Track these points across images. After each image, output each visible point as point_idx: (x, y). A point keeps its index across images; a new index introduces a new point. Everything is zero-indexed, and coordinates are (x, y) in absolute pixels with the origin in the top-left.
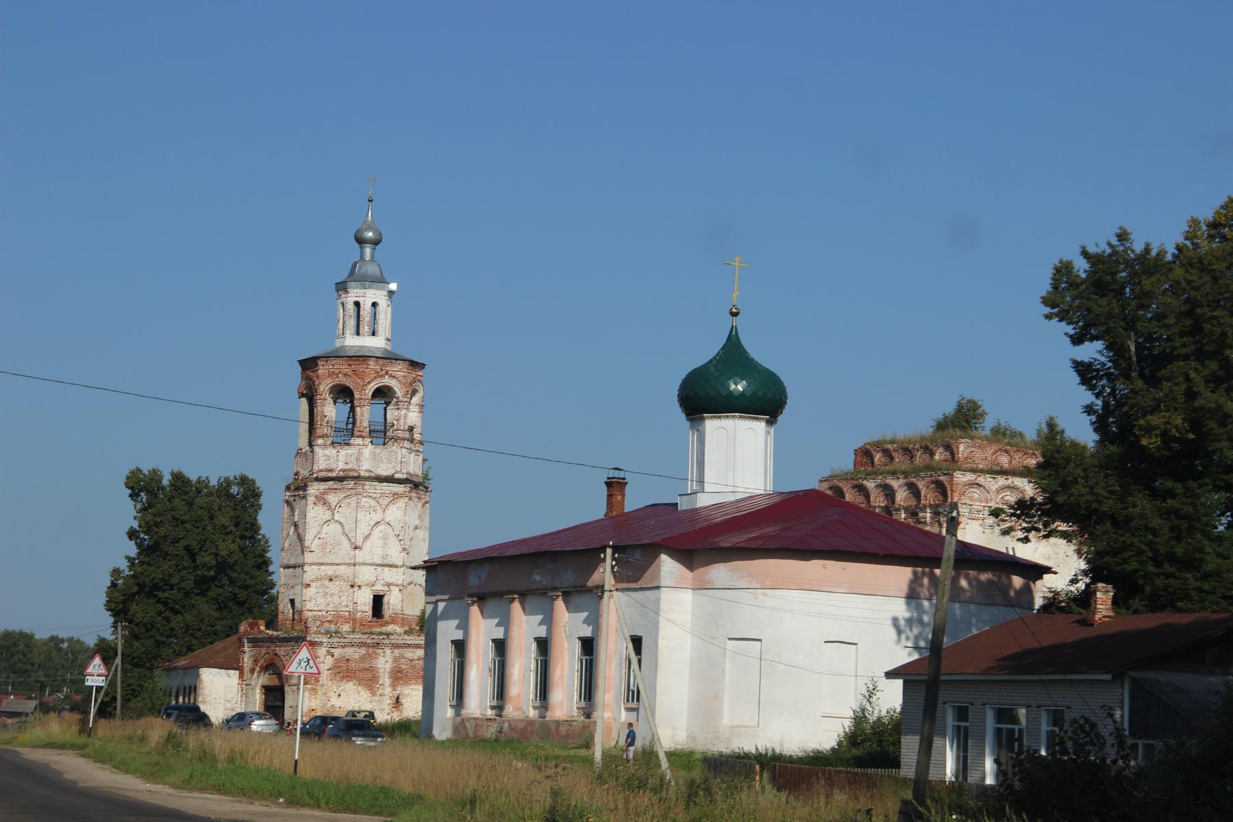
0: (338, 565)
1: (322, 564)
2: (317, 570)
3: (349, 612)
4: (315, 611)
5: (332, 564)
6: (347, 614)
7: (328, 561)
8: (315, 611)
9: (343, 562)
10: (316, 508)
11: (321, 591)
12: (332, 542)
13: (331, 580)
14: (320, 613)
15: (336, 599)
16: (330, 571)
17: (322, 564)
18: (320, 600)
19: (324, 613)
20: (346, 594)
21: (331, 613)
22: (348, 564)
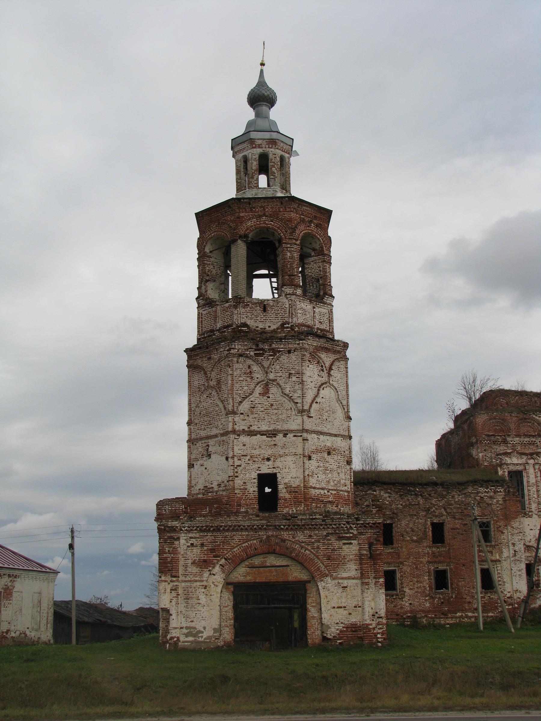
0: (336, 436)
1: (322, 433)
2: (316, 440)
3: (348, 492)
4: (318, 489)
5: (331, 435)
6: (346, 494)
7: (325, 430)
8: (318, 489)
9: (339, 433)
10: (310, 366)
11: (322, 465)
12: (328, 408)
13: (329, 453)
14: (322, 492)
15: (335, 474)
16: (328, 442)
17: (322, 433)
18: (322, 477)
19: (326, 491)
20: (343, 471)
21: (333, 492)
22: (342, 436)
